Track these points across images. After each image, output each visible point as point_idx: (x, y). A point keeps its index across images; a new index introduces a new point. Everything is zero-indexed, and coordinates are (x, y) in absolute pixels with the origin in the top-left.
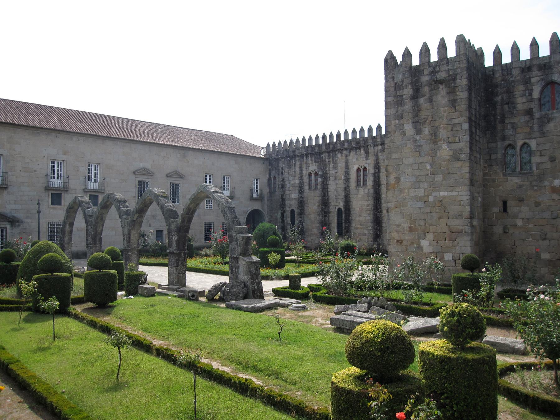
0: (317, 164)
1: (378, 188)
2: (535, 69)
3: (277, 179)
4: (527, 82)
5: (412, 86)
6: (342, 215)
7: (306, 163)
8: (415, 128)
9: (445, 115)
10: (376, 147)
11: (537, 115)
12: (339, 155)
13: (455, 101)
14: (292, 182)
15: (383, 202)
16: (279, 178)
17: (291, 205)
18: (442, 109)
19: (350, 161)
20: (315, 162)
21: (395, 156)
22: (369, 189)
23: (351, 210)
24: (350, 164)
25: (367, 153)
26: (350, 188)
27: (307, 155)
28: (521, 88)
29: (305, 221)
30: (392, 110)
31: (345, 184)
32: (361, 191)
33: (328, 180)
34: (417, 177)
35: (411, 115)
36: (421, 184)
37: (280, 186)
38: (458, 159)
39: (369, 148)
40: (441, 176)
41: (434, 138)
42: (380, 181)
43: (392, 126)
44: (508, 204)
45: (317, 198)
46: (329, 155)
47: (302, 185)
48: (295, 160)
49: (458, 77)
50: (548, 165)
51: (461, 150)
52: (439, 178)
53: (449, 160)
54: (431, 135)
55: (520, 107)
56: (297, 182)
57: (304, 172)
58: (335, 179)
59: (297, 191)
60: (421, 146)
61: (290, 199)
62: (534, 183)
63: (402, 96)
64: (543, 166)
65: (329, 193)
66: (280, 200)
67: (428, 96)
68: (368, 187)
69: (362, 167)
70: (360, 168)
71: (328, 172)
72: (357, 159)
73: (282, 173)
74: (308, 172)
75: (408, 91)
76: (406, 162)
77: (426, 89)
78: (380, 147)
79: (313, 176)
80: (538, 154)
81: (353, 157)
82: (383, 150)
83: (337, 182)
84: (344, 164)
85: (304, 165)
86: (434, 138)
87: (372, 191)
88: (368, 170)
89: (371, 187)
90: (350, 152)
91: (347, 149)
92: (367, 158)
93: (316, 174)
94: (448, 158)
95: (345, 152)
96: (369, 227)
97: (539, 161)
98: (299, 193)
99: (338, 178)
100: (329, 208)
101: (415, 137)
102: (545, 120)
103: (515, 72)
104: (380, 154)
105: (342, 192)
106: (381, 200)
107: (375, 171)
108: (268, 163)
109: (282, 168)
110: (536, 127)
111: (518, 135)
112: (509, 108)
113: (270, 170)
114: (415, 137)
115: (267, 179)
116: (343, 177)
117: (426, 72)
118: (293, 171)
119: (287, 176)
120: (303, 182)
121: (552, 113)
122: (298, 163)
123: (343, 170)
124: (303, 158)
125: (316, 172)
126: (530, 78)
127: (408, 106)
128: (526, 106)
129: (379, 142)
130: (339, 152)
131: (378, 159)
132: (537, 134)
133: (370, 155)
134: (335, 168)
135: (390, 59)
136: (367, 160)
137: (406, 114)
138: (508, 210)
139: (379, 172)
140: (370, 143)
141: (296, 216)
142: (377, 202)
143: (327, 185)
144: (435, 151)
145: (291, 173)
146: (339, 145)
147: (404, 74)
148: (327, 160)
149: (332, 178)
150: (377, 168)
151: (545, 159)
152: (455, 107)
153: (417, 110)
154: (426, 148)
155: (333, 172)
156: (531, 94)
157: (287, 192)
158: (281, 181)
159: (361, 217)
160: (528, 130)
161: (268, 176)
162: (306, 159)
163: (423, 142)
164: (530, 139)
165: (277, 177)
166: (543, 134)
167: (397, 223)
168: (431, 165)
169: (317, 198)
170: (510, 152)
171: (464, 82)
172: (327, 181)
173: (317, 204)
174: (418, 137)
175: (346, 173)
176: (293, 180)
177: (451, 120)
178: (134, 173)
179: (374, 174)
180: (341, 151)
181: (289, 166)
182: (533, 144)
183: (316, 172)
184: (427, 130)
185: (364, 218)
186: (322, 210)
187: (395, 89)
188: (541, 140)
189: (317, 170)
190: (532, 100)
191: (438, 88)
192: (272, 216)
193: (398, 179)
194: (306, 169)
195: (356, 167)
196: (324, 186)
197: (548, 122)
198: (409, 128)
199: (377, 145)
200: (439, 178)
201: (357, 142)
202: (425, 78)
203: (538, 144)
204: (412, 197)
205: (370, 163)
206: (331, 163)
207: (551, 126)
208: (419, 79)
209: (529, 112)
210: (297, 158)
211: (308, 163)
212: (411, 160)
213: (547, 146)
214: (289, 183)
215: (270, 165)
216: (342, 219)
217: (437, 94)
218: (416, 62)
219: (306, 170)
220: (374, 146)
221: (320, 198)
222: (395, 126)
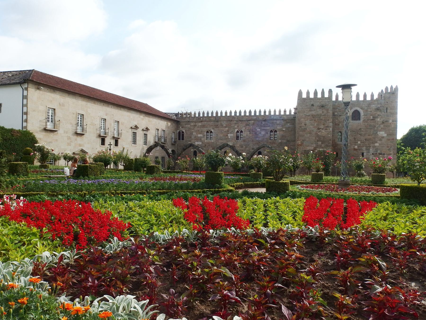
9: (323, 119)
40: (321, 142)
44: (339, 154)
52: (320, 143)
79: (209, 133)
135: (300, 93)
138: (339, 156)
170: (340, 134)
178: (131, 128)
195: (236, 130)
200: (320, 143)
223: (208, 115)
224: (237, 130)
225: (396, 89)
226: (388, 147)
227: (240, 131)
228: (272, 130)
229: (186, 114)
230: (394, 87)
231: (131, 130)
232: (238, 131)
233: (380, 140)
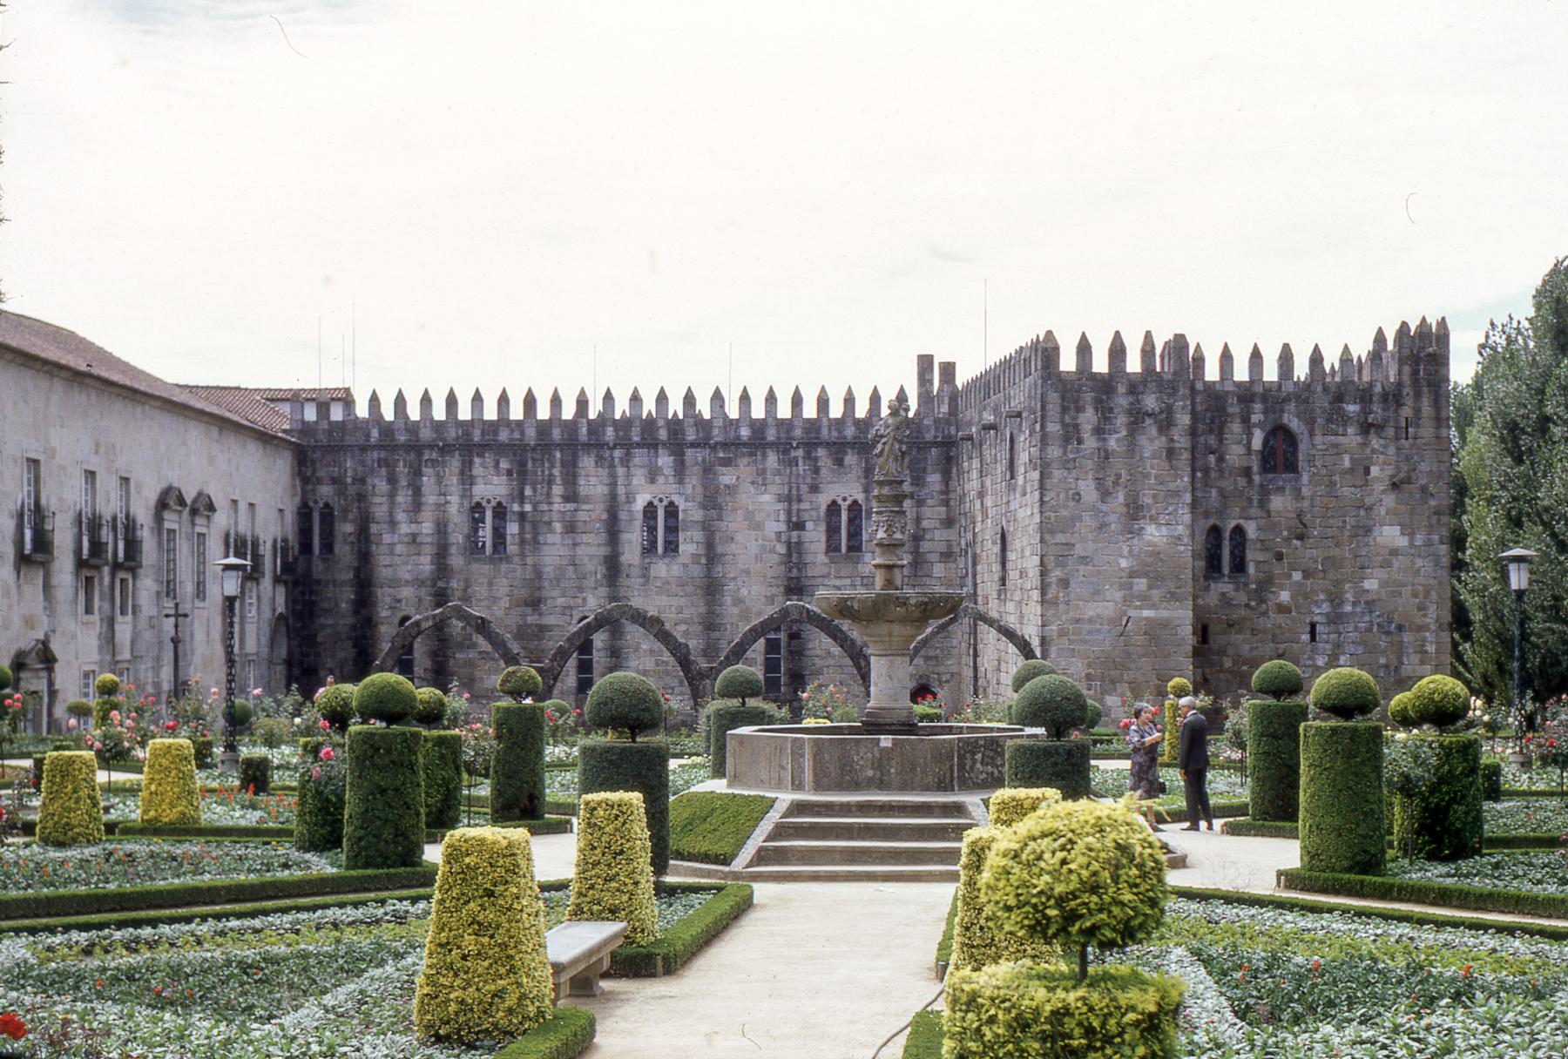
4: (1246, 420)
15: (728, 600)
17: (399, 601)
22: (685, 566)
32: (662, 569)
40: (1144, 581)
56: (427, 528)
58: (571, 528)
61: (395, 583)
69: (661, 500)
70: (656, 502)
75: (1088, 418)
77: (1121, 420)
93: (500, 512)
117: (1121, 389)
136: (681, 482)
138: (1211, 638)
164: (1246, 519)
182: (1251, 529)
193: (1065, 583)
195: (640, 502)
198: (1088, 489)
202: (1122, 400)
209: (1247, 472)
226: (1415, 595)
230: (1433, 321)
232: (650, 504)
233: (1386, 564)
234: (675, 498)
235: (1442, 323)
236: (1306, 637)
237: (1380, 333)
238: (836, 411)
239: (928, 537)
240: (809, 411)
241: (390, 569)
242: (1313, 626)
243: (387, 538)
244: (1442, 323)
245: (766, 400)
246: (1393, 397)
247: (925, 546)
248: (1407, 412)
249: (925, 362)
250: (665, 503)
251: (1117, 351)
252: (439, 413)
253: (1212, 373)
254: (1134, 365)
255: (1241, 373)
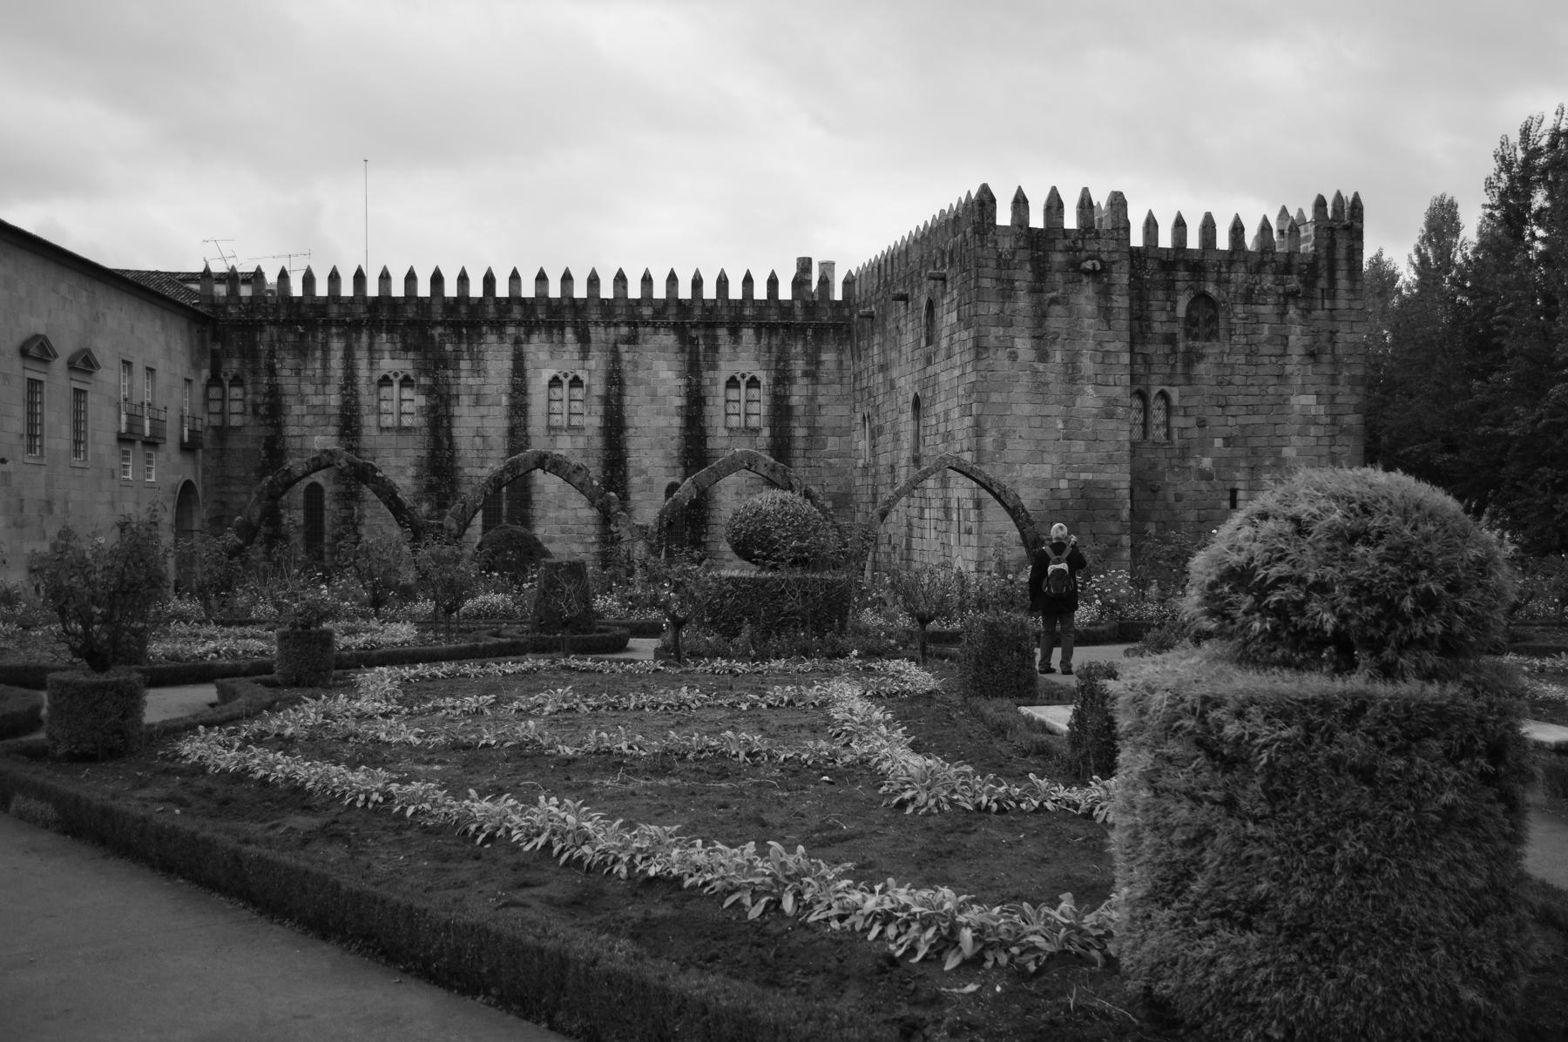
0: (411, 355)
1: (618, 436)
2: (1181, 267)
3: (249, 387)
5: (1032, 266)
6: (500, 503)
7: (371, 349)
8: (1037, 348)
9: (1092, 332)
10: (612, 329)
11: (1181, 346)
12: (492, 338)
13: (1108, 309)
14: (317, 400)
15: (631, 472)
16: (255, 383)
18: (1087, 322)
19: (530, 356)
20: (406, 349)
21: (995, 397)
23: (534, 489)
24: (528, 365)
25: (584, 339)
26: (530, 429)
27: (375, 326)
28: (1160, 294)
29: (367, 521)
30: (992, 305)
31: (510, 417)
33: (453, 402)
34: (1038, 441)
35: (1028, 322)
36: (1045, 455)
37: (262, 410)
38: (1110, 416)
39: (592, 330)
40: (1082, 443)
41: (1072, 374)
42: (624, 417)
43: (991, 338)
45: (411, 452)
46: (460, 335)
47: (352, 411)
48: (328, 336)
49: (1115, 267)
50: (1195, 433)
51: (1117, 401)
52: (1079, 446)
53: (1096, 416)
54: (1066, 365)
55: (1157, 327)
56: (334, 400)
57: (363, 371)
58: (478, 400)
59: (333, 430)
60: (1047, 384)
62: (1175, 462)
63: (1011, 281)
64: (1188, 434)
65: (457, 440)
66: (263, 453)
67: (1061, 291)
68: (589, 432)
69: (566, 375)
70: (561, 377)
71: (451, 381)
72: (552, 354)
73: (272, 371)
74: (377, 376)
76: (1017, 411)
78: (624, 330)
80: (1182, 413)
81: (538, 350)
82: (632, 340)
83: (483, 410)
84: (508, 364)
85: (362, 358)
86: (1072, 374)
87: (598, 442)
88: (588, 387)
89: (597, 431)
90: (529, 333)
91: (519, 324)
92: (585, 357)
94: (1095, 411)
95: (511, 330)
96: (590, 536)
97: (1182, 425)
98: (341, 435)
99: (490, 400)
100: (454, 483)
101: (1035, 365)
102: (1192, 358)
103: (1151, 264)
104: (623, 348)
105: (500, 440)
106: (626, 466)
107: (608, 390)
108: (208, 336)
109: (272, 354)
110: (1179, 368)
111: (1154, 377)
112: (1141, 326)
113: (214, 354)
114: (1035, 365)
115: (203, 381)
116: (505, 400)
117: (1060, 246)
118: (318, 365)
119: (294, 380)
120: (358, 404)
121: (1203, 347)
122: (337, 346)
123: (506, 381)
124: (359, 333)
125: (407, 378)
126: (1174, 281)
127: (1023, 303)
128: (1166, 329)
129: (623, 318)
130: (491, 329)
131: (616, 358)
132: (1181, 379)
133: (593, 347)
134: (478, 371)
135: (985, 200)
136: (584, 358)
137: (1019, 318)
139: (620, 395)
140: (594, 317)
141: (326, 503)
142: (612, 471)
143: (450, 417)
144: (1072, 396)
145: (310, 373)
146: (491, 309)
147: (1018, 240)
148: (449, 347)
149: (465, 400)
150: (615, 384)
151: (1192, 422)
152: (1108, 321)
153: (1040, 317)
154: (1056, 388)
155: (471, 381)
156: (1174, 309)
157: (292, 430)
158: (265, 395)
159: (563, 511)
160: (1168, 370)
161: (206, 373)
162: (371, 337)
163: (1051, 377)
164: (1170, 385)
165: (248, 378)
166: (1189, 379)
167: (998, 528)
168: (1065, 422)
169: (411, 452)
170: (1137, 403)
171: (1125, 279)
172: (448, 405)
173: (411, 471)
174: (1041, 367)
175: (515, 390)
176: (316, 394)
177: (1100, 343)
179: (606, 400)
180: (498, 326)
181: (302, 351)
182: (1175, 394)
183: (407, 378)
184: (1058, 356)
185: (571, 513)
186: (431, 488)
187: (998, 267)
188: (1186, 389)
189: (411, 373)
190: (1173, 319)
191: (1080, 281)
192: (224, 504)
193: (1001, 446)
194: (371, 364)
195: (547, 375)
196: (436, 419)
197: (1198, 361)
198: (1023, 345)
199: (616, 325)
200: (1079, 446)
201: (553, 307)
202: (1058, 258)
203: (1182, 396)
204: (1029, 479)
205: (593, 367)
206: (466, 355)
207: (1201, 368)
208: (1046, 255)
209: (1170, 339)
210: (334, 330)
211: (377, 346)
212: (1027, 409)
213: (1194, 401)
214: (302, 403)
215: (215, 339)
216: (500, 515)
217: (1078, 293)
218: (1037, 221)
219: (371, 370)
220: (607, 326)
221: (424, 453)
222: (996, 338)
223: (389, 289)
224: (553, 372)
225: (1357, 207)
227: (566, 382)
228: (733, 379)
229: (232, 278)
230: (1348, 195)
231: (18, 363)
234: (579, 373)
235: (1356, 197)
236: (1226, 504)
237: (1265, 219)
238: (735, 292)
239: (823, 412)
240: (709, 292)
241: (299, 440)
242: (1234, 492)
243: (297, 409)
244: (1356, 197)
245: (668, 281)
246: (1311, 271)
247: (821, 421)
248: (1322, 283)
249: (805, 265)
250: (570, 378)
251: (1054, 205)
252: (347, 290)
253: (1137, 239)
254: (1071, 221)
255: (1165, 240)
